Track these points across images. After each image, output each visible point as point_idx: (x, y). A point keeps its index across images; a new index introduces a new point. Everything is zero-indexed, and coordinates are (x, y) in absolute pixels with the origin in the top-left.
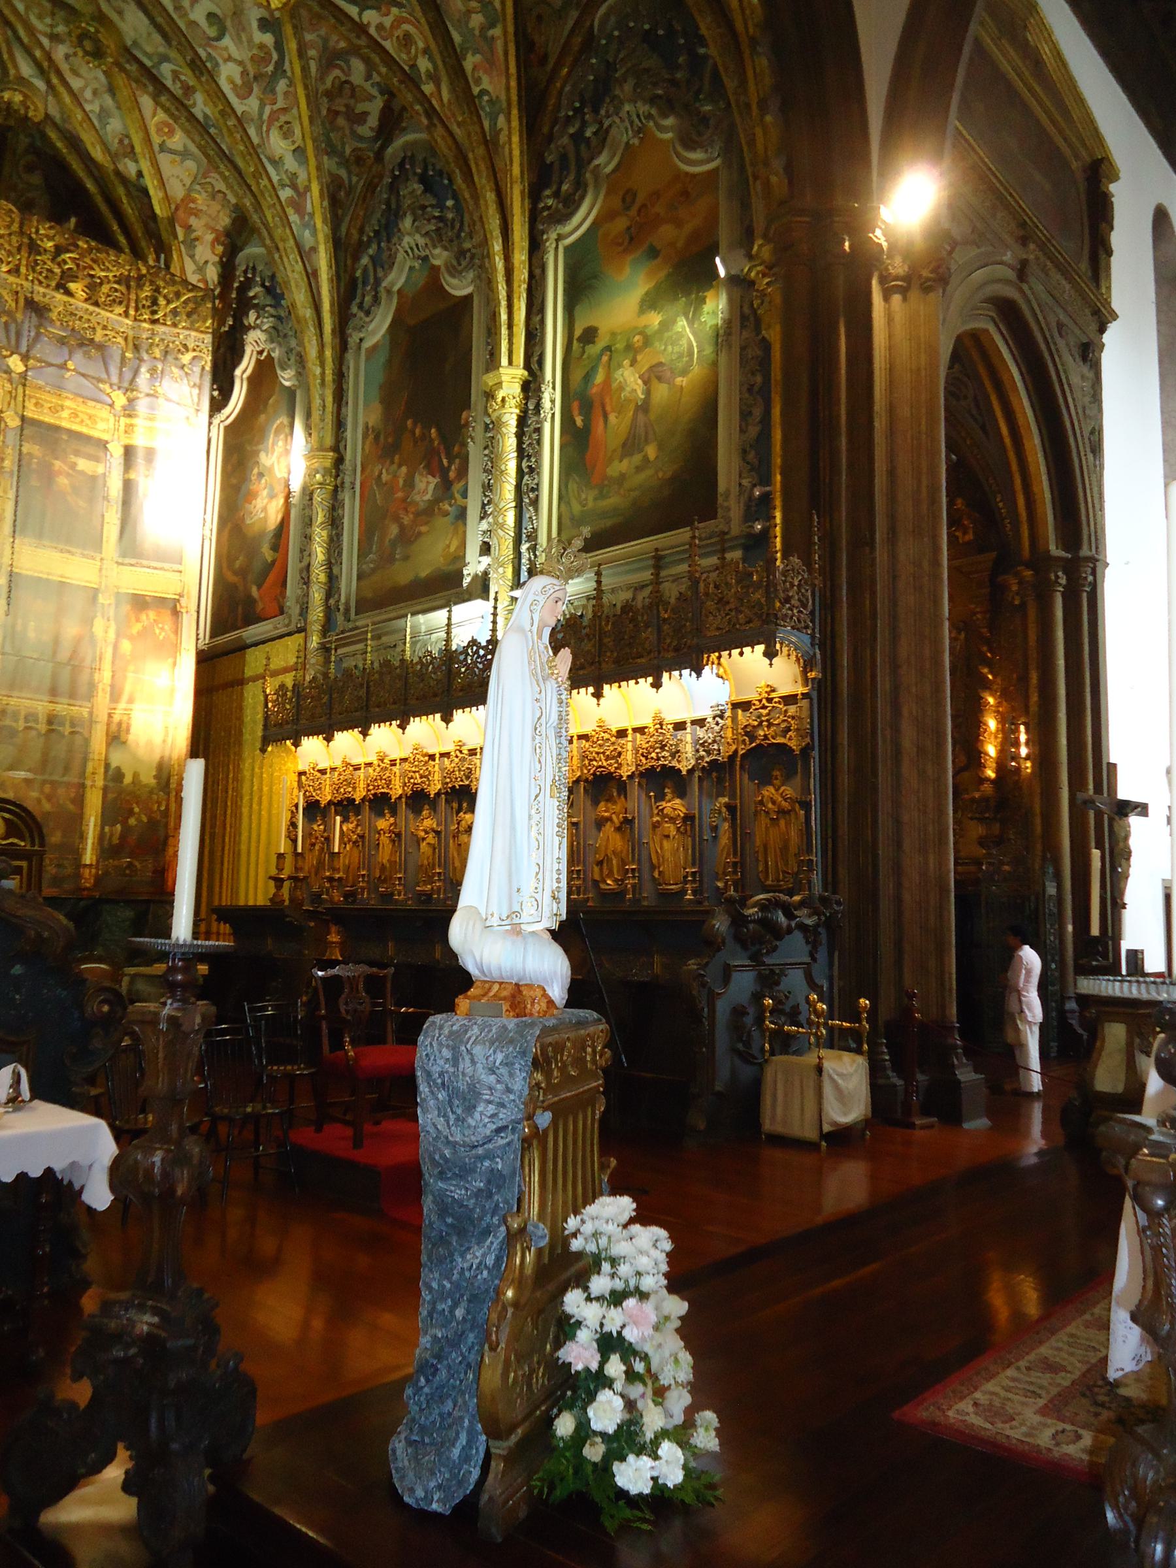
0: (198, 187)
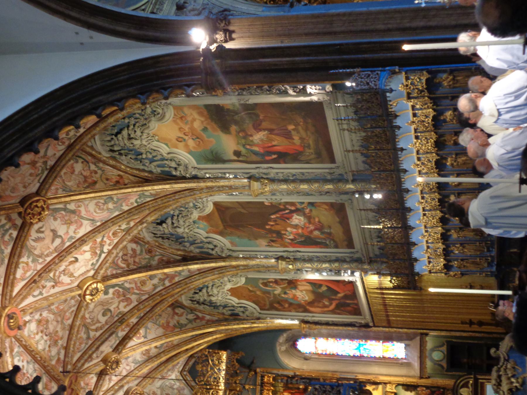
0: (158, 322)
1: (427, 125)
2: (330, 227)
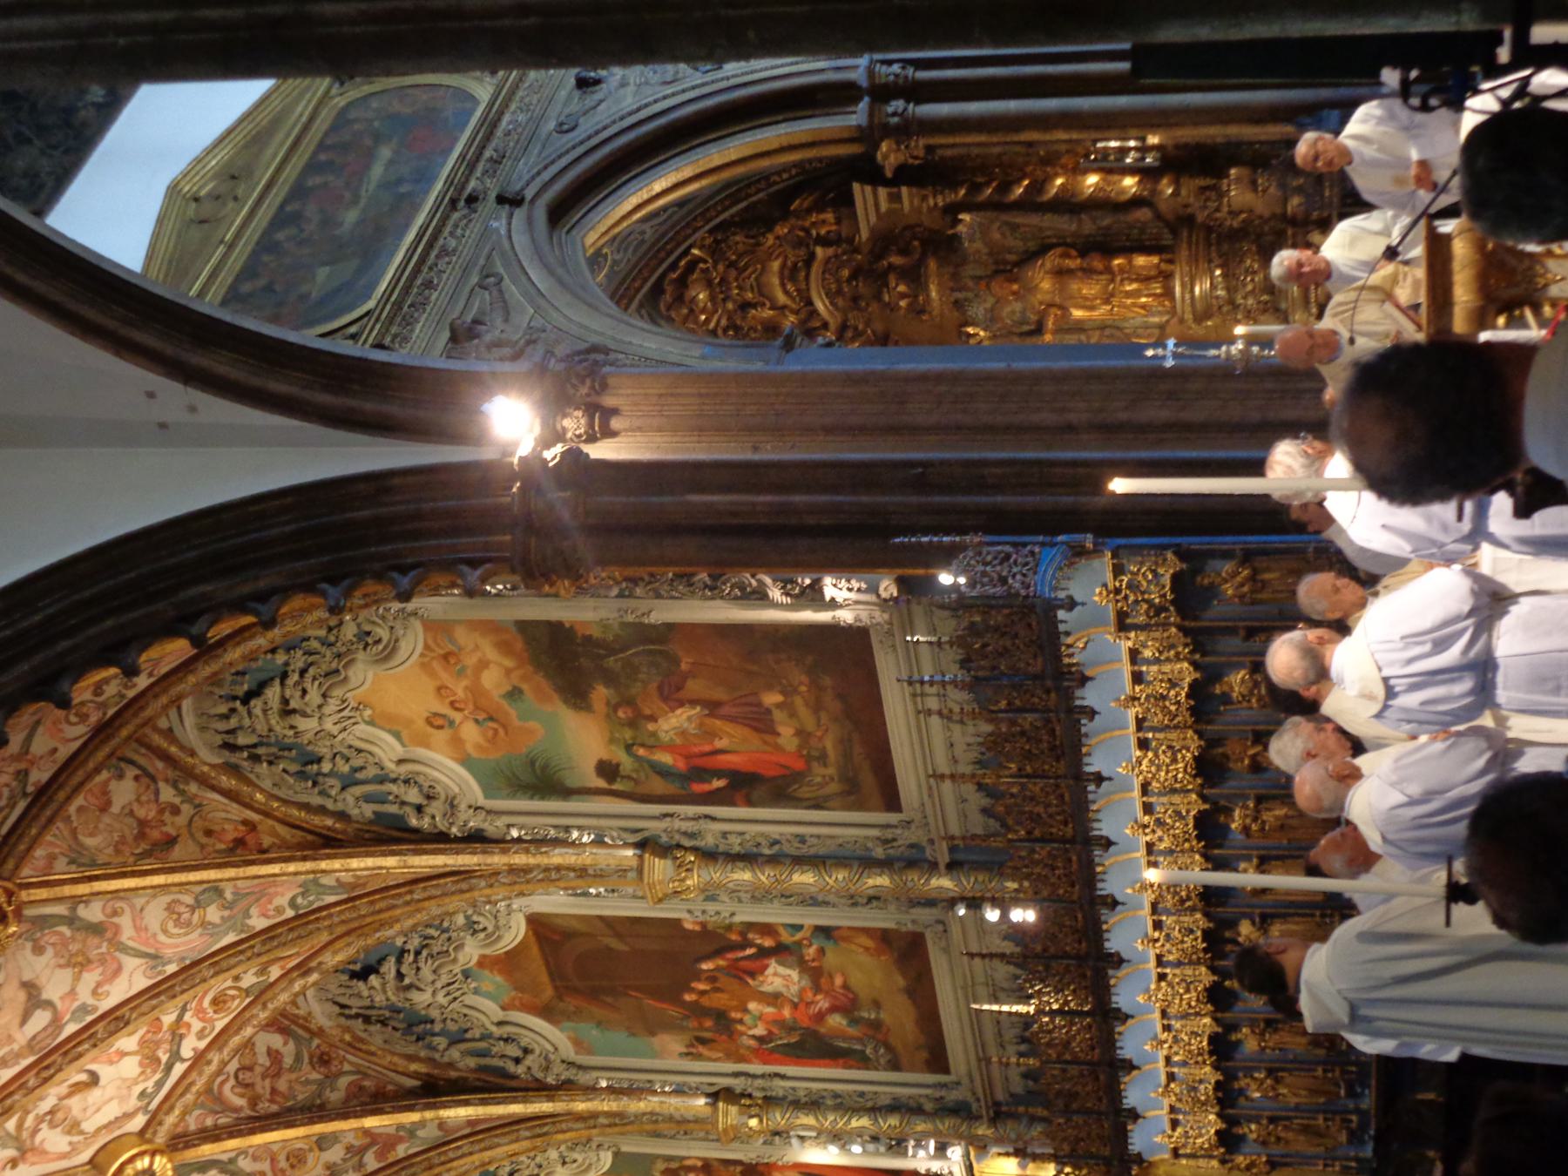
1: (1173, 708)
2: (877, 1005)
